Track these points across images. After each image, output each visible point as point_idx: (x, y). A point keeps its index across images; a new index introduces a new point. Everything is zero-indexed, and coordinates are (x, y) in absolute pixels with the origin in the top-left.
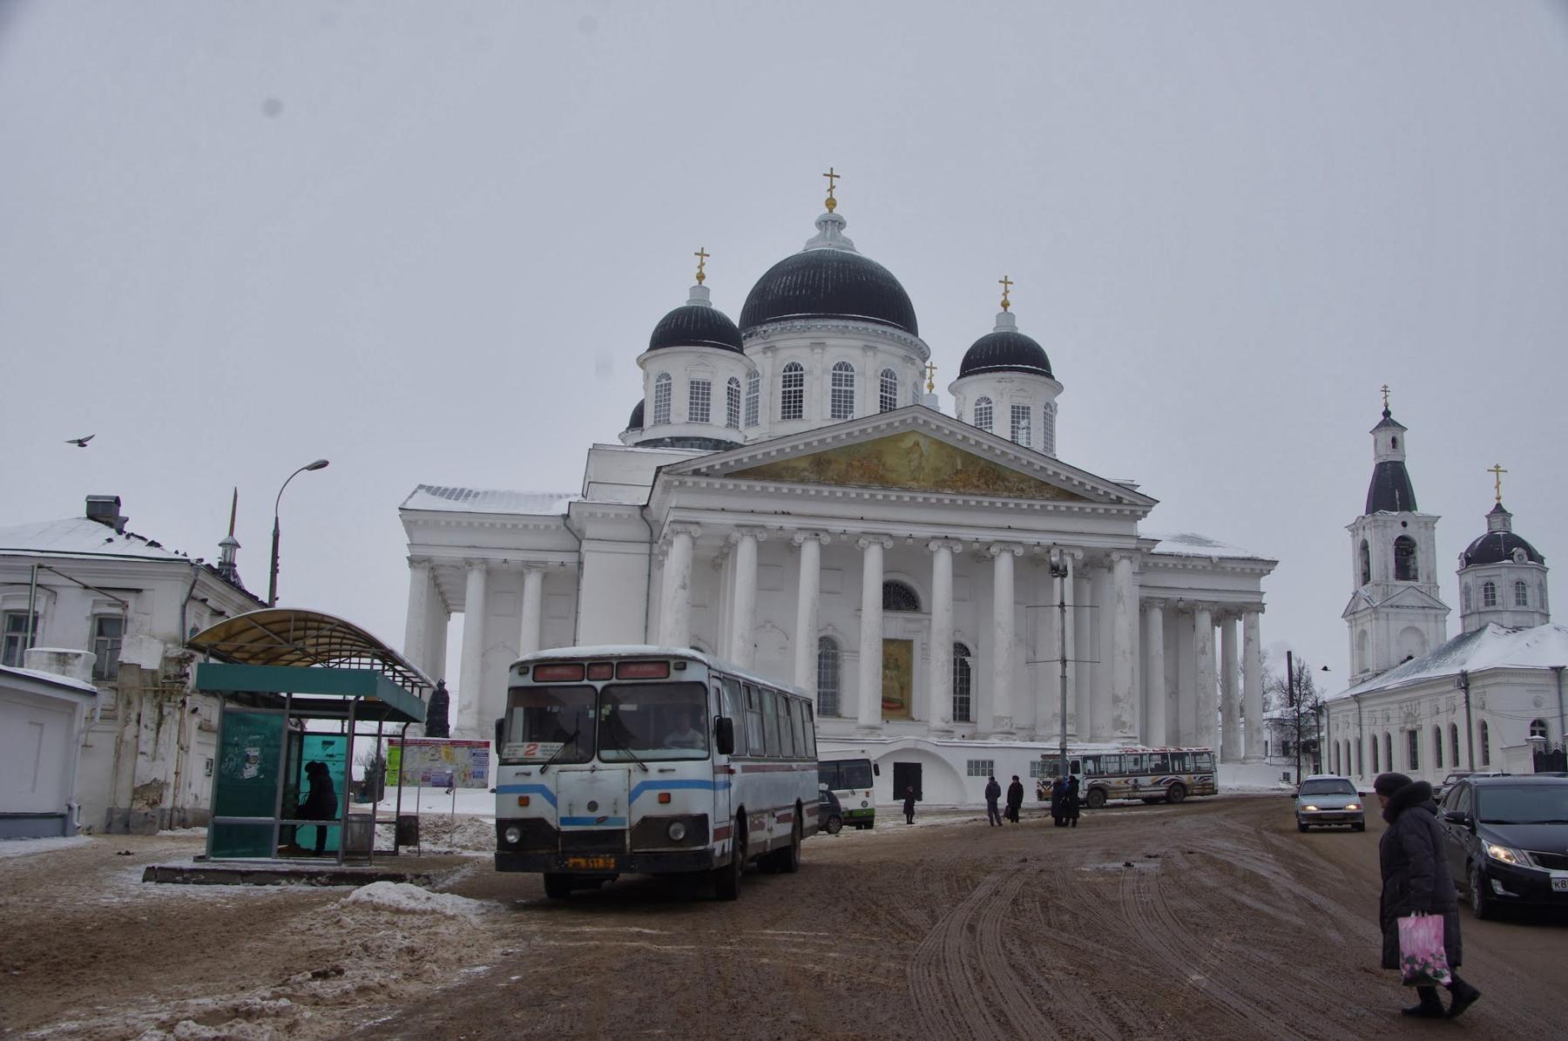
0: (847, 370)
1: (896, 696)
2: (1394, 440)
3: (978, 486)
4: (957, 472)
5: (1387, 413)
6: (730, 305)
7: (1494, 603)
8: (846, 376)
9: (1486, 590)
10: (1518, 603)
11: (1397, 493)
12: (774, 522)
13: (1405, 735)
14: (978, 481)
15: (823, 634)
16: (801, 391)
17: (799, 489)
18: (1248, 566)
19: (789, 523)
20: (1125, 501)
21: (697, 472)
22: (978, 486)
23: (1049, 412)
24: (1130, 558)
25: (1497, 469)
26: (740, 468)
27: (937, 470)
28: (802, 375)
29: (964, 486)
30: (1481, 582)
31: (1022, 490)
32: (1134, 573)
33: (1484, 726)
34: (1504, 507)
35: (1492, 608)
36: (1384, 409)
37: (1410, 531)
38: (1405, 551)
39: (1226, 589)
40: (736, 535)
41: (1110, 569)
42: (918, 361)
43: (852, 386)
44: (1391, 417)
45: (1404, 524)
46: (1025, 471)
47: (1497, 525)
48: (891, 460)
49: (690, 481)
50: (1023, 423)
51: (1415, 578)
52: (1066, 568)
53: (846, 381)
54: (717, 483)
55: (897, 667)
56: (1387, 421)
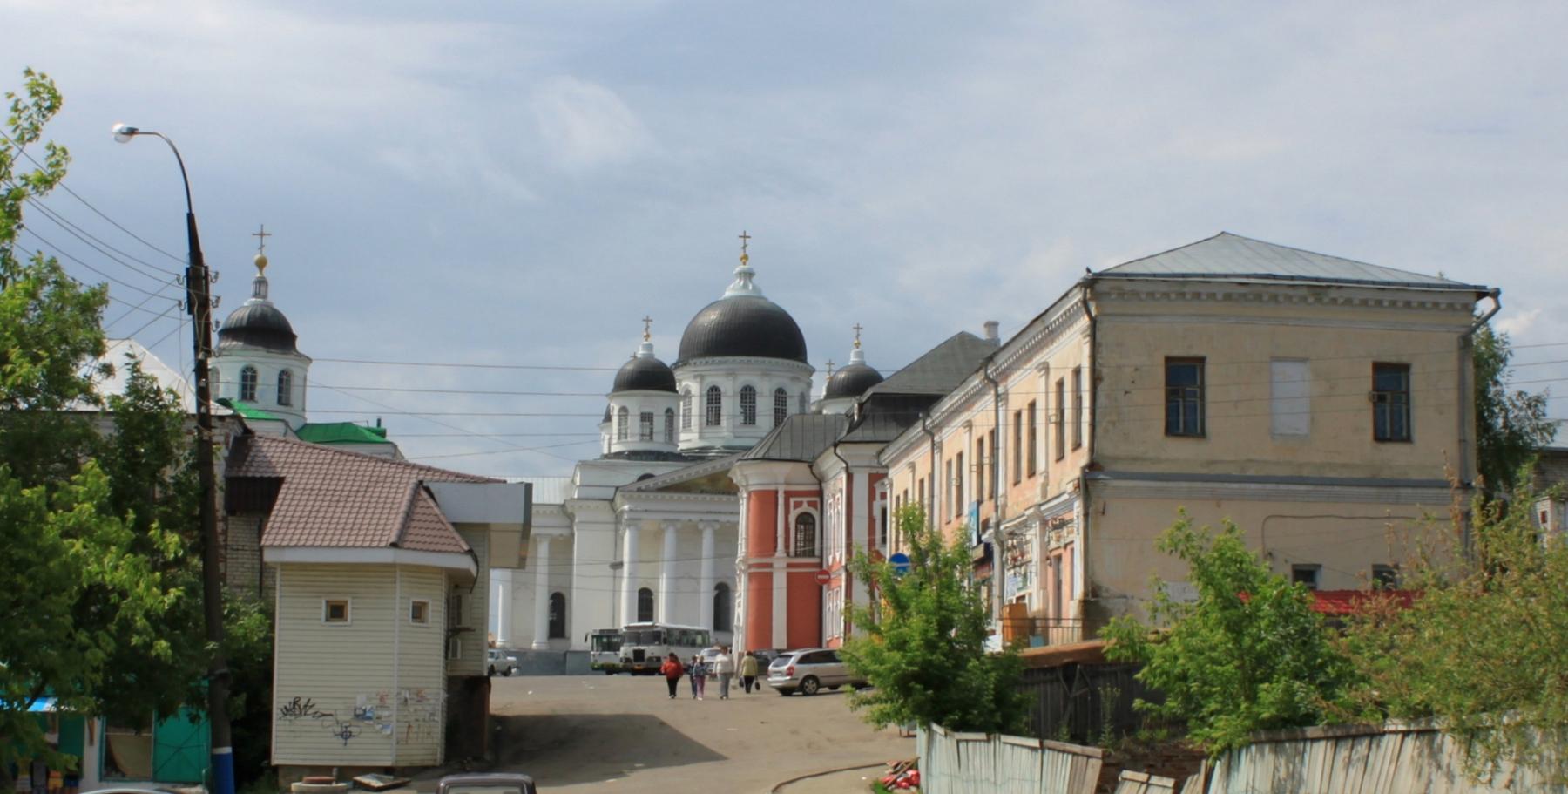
6: (667, 352)
12: (685, 517)
15: (719, 581)
17: (700, 497)
19: (695, 518)
26: (665, 485)
40: (663, 526)
49: (636, 495)
54: (652, 495)
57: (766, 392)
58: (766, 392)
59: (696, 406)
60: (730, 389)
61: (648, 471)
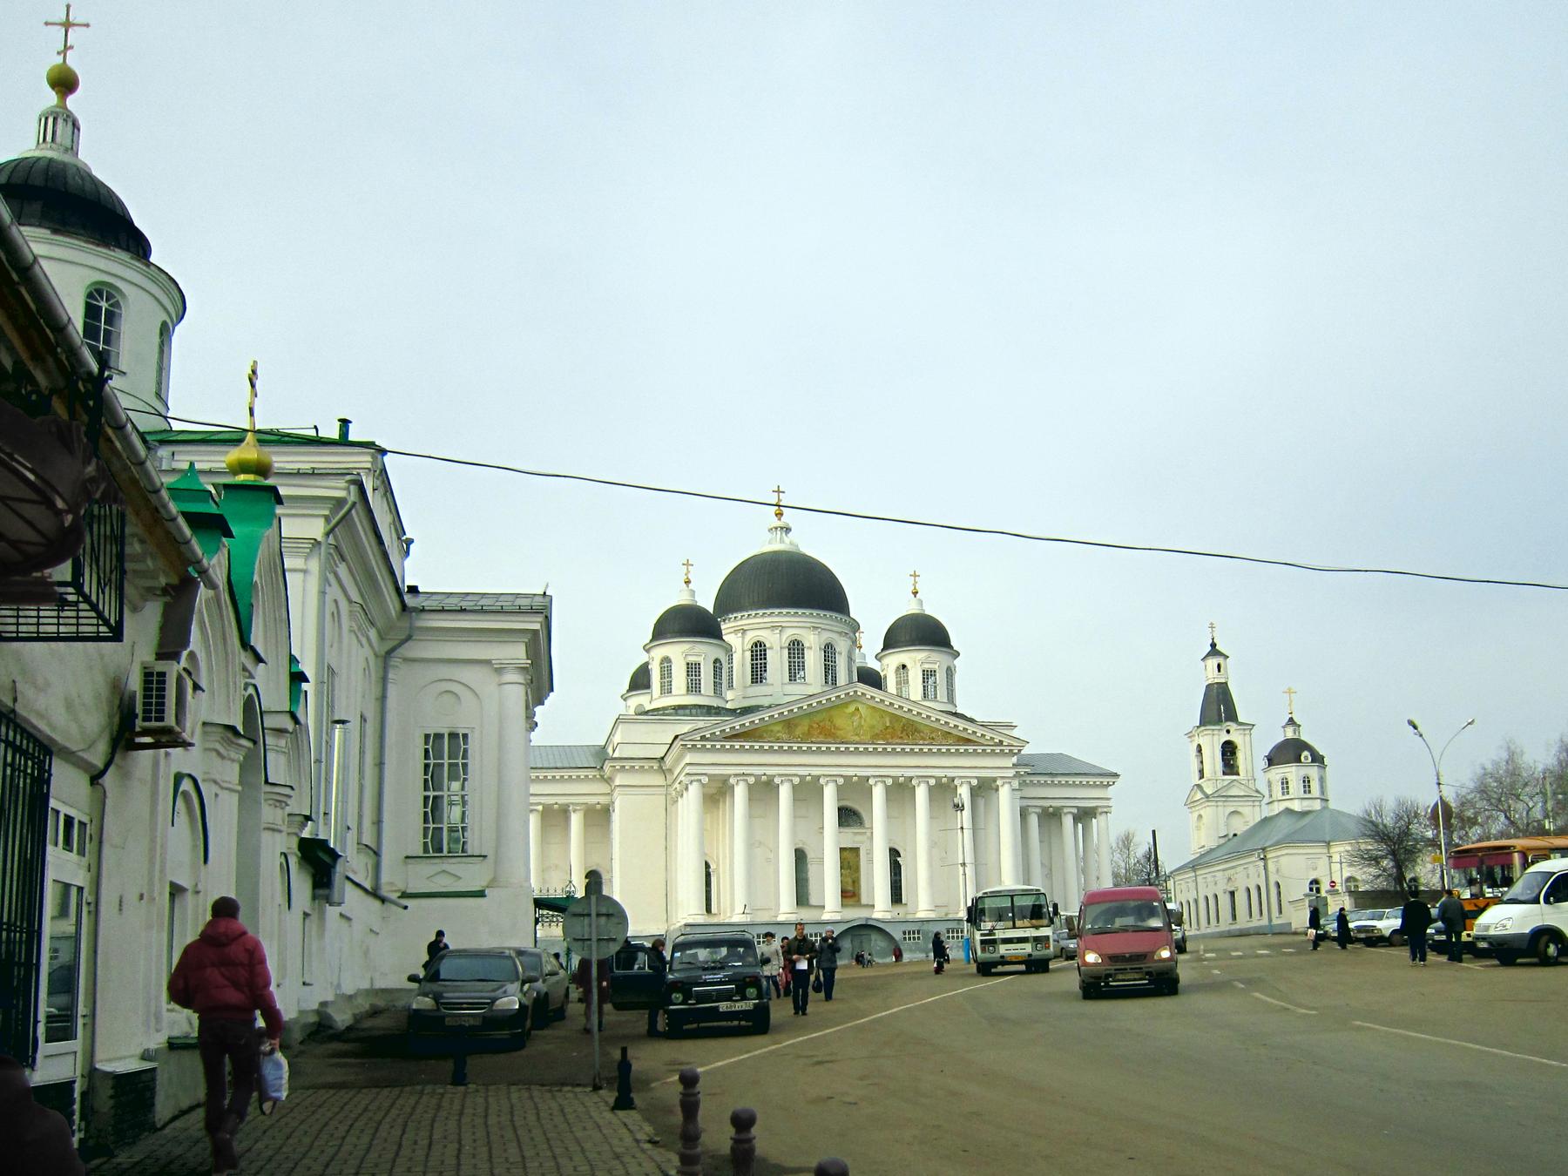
1: (850, 888)
2: (1219, 666)
3: (901, 737)
4: (887, 727)
5: (1213, 645)
7: (1288, 793)
9: (1282, 783)
10: (1305, 792)
11: (1222, 707)
13: (1228, 896)
14: (902, 733)
18: (1098, 780)
20: (1004, 744)
21: (703, 738)
22: (901, 737)
23: (950, 672)
24: (1010, 783)
25: (1289, 692)
27: (872, 727)
28: (765, 650)
29: (892, 738)
30: (1279, 777)
31: (933, 739)
32: (1013, 790)
33: (1278, 885)
34: (1295, 719)
35: (1287, 797)
36: (1211, 641)
37: (1232, 737)
38: (1229, 750)
39: (1086, 796)
41: (997, 790)
42: (852, 635)
44: (1217, 647)
45: (1228, 732)
46: (935, 725)
47: (1290, 734)
48: (839, 722)
49: (699, 745)
50: (931, 681)
51: (1238, 774)
52: (963, 806)
55: (850, 868)
56: (1214, 651)
57: (813, 643)
58: (813, 643)
59: (741, 662)
60: (777, 645)
61: (701, 725)
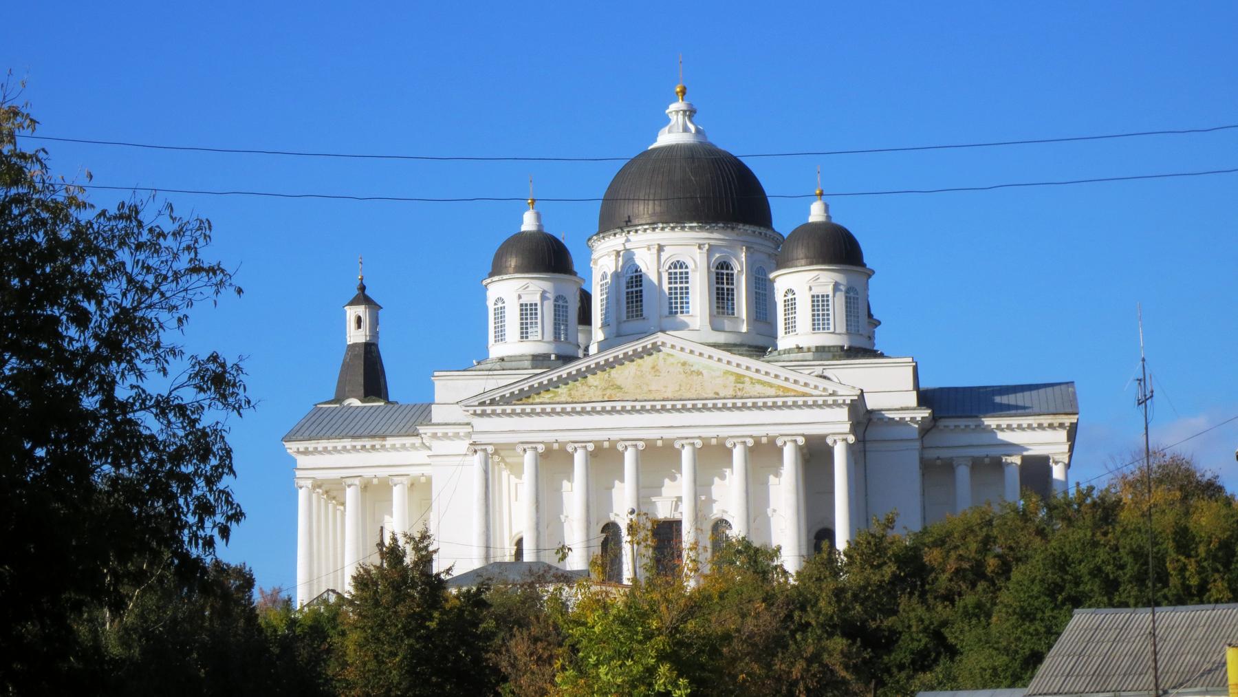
0: (681, 267)
8: (681, 273)
16: (641, 291)
43: (687, 282)
53: (681, 278)
